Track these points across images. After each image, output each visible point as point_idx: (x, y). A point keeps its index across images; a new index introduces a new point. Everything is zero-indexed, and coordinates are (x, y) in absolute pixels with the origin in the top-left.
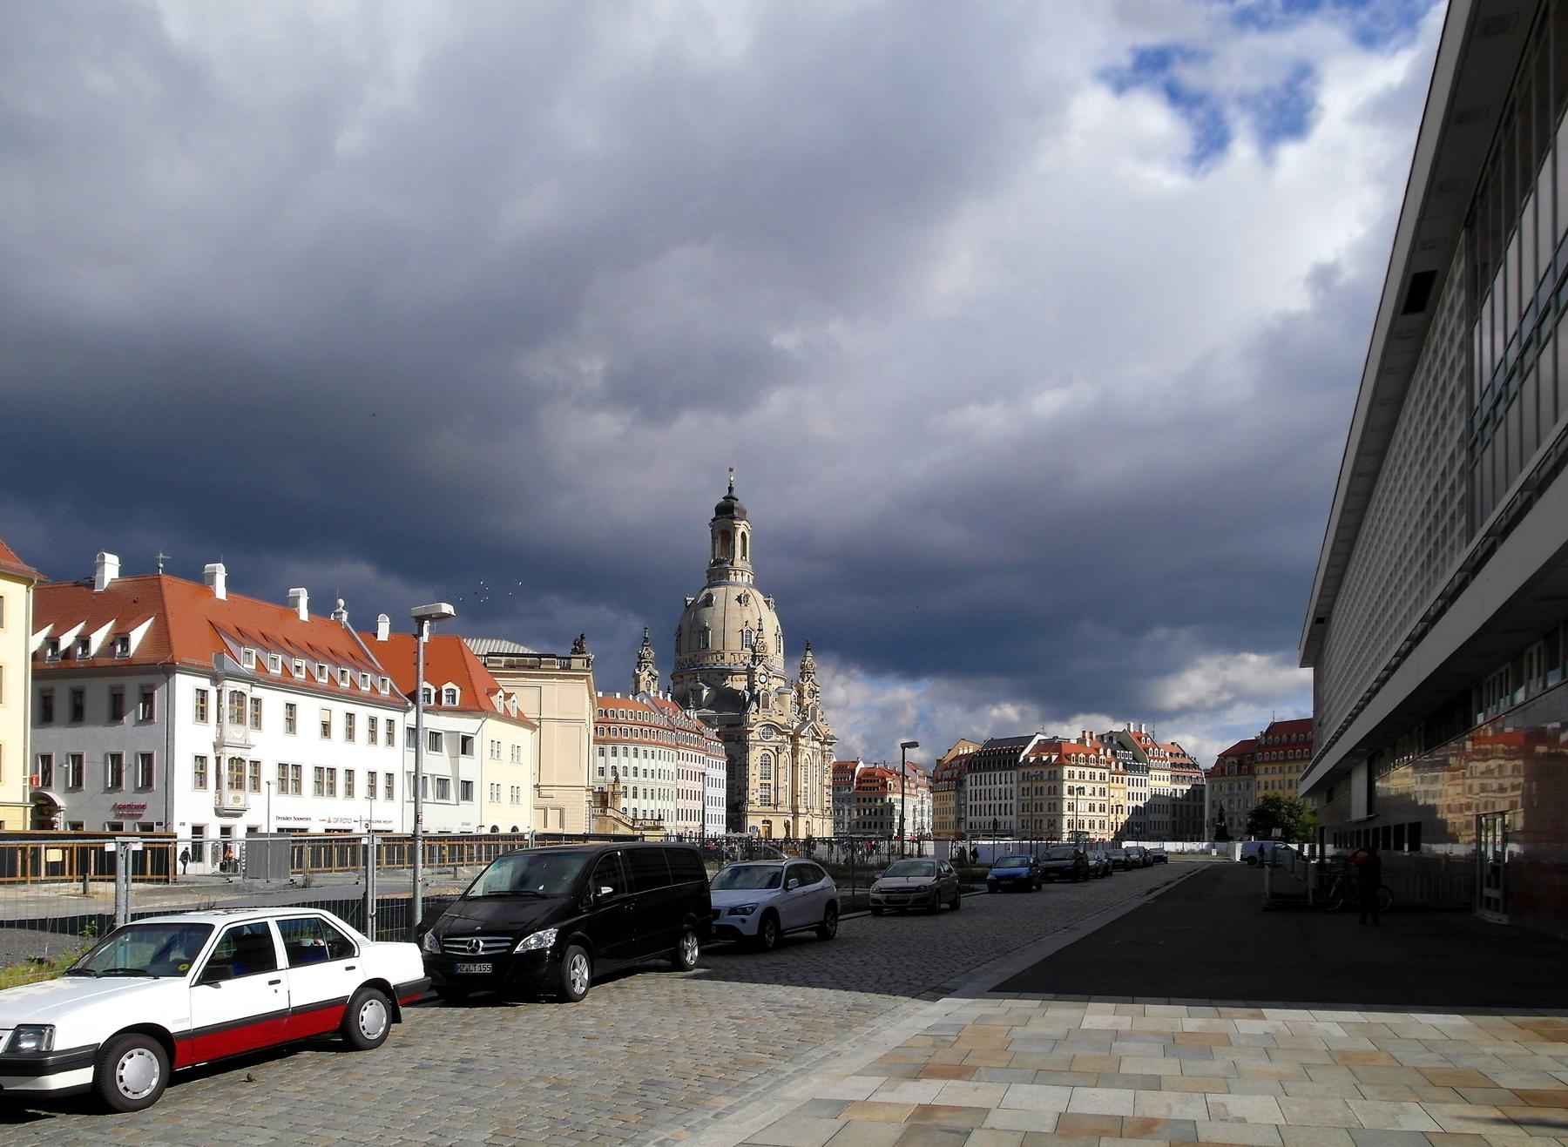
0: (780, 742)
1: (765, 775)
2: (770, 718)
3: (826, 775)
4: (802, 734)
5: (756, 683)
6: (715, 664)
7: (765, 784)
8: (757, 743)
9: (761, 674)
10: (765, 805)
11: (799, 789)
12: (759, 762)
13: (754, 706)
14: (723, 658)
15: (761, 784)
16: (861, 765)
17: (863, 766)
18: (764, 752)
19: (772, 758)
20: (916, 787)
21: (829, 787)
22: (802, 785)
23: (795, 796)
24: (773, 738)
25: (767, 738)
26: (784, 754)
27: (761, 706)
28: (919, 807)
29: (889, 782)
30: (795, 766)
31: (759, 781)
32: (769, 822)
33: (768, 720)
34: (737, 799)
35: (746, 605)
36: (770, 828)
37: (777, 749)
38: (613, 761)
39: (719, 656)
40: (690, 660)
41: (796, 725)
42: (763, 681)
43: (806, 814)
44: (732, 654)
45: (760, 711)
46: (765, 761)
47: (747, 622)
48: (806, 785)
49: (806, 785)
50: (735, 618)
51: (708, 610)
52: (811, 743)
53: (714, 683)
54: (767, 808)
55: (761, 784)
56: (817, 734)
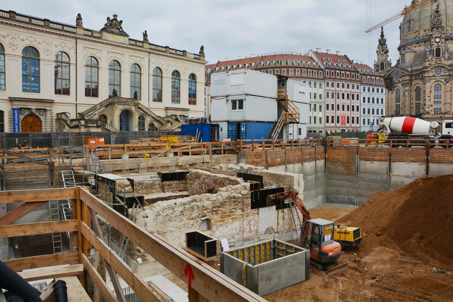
1: (438, 96)
2: (440, 62)
5: (433, 43)
6: (415, 38)
8: (432, 78)
9: (436, 38)
12: (433, 89)
14: (419, 34)
18: (437, 83)
24: (442, 74)
25: (438, 74)
33: (439, 63)
37: (445, 81)
39: (417, 33)
40: (404, 39)
44: (425, 31)
45: (433, 59)
46: (438, 88)
55: (435, 102)
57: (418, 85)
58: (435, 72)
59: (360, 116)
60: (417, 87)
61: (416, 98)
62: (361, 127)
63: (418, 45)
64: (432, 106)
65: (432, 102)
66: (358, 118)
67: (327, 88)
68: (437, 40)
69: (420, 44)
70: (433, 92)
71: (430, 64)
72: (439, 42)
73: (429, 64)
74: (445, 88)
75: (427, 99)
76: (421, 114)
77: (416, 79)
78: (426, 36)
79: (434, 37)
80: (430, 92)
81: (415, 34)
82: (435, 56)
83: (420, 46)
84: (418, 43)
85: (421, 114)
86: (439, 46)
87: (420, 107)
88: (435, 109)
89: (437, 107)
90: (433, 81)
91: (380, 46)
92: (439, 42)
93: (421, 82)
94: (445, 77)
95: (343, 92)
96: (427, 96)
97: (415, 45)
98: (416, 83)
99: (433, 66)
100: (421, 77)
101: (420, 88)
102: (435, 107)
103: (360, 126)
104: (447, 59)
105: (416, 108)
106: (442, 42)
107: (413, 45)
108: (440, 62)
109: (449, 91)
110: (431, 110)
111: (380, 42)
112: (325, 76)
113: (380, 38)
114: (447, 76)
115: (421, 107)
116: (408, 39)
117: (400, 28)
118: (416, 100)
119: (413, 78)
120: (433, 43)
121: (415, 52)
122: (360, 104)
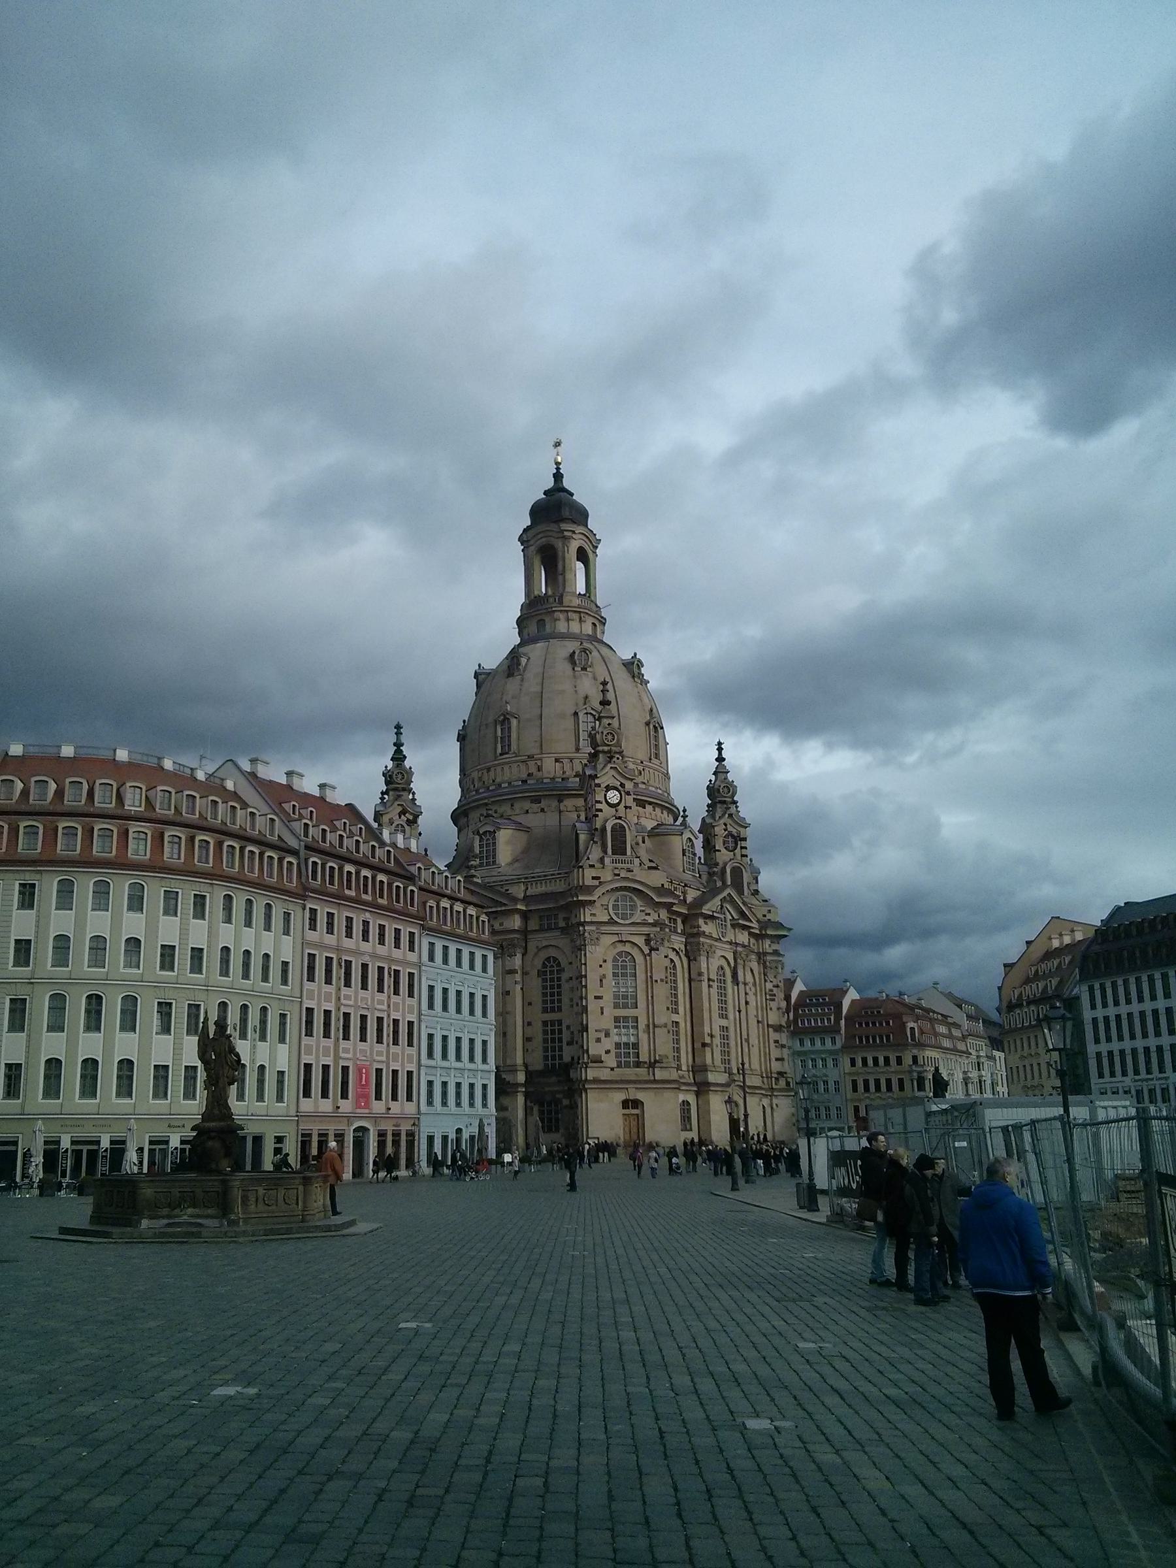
0: (654, 925)
1: (625, 997)
2: (629, 875)
3: (774, 1005)
4: (706, 910)
5: (598, 806)
6: (524, 782)
7: (626, 1018)
8: (604, 928)
9: (608, 788)
10: (627, 1065)
11: (707, 1029)
12: (608, 969)
13: (595, 853)
14: (539, 769)
15: (617, 1019)
16: (852, 995)
17: (857, 996)
19: (639, 959)
20: (964, 1038)
21: (778, 1028)
22: (713, 1024)
23: (699, 1045)
24: (638, 917)
26: (663, 951)
27: (609, 851)
28: (974, 1075)
29: (911, 1025)
30: (693, 980)
31: (610, 1012)
32: (637, 1104)
34: (567, 1054)
35: (584, 669)
36: (640, 1120)
37: (648, 942)
38: (61, 922)
39: (531, 763)
40: (480, 779)
41: (692, 895)
42: (615, 801)
43: (728, 1085)
44: (557, 760)
45: (607, 860)
46: (623, 967)
47: (586, 697)
48: (724, 1023)
49: (724, 1023)
50: (562, 692)
51: (512, 685)
52: (730, 936)
53: (518, 819)
54: (630, 1073)
55: (617, 1019)
56: (743, 915)
57: (552, 953)
58: (615, 907)
59: (419, 1065)
60: (548, 959)
61: (545, 1002)
62: (422, 1118)
63: (535, 806)
64: (607, 1035)
65: (607, 1022)
66: (410, 1073)
67: (312, 936)
68: (613, 797)
69: (543, 804)
70: (610, 981)
71: (598, 878)
72: (618, 804)
73: (593, 878)
74: (649, 969)
75: (593, 1006)
76: (567, 1067)
77: (541, 930)
78: (563, 779)
79: (603, 786)
80: (601, 981)
81: (523, 767)
82: (609, 851)
83: (542, 810)
84: (536, 800)
85: (567, 1067)
86: (620, 818)
87: (560, 1040)
88: (618, 1045)
89: (624, 1039)
90: (607, 940)
91: (391, 793)
92: (618, 804)
93: (563, 942)
94: (646, 930)
95: (366, 959)
96: (591, 997)
97: (527, 805)
98: (545, 943)
99: (609, 888)
100: (562, 924)
101: (559, 964)
102: (616, 1039)
103: (419, 1113)
104: (650, 868)
105: (545, 1041)
106: (626, 807)
107: (517, 806)
108: (629, 875)
109: (662, 980)
110: (608, 1052)
111: (388, 777)
112: (303, 880)
113: (390, 765)
114: (654, 925)
115: (566, 1036)
116: (498, 780)
117: (462, 738)
118: (545, 1010)
119: (533, 925)
120: (598, 806)
121: (527, 830)
122: (420, 1014)
